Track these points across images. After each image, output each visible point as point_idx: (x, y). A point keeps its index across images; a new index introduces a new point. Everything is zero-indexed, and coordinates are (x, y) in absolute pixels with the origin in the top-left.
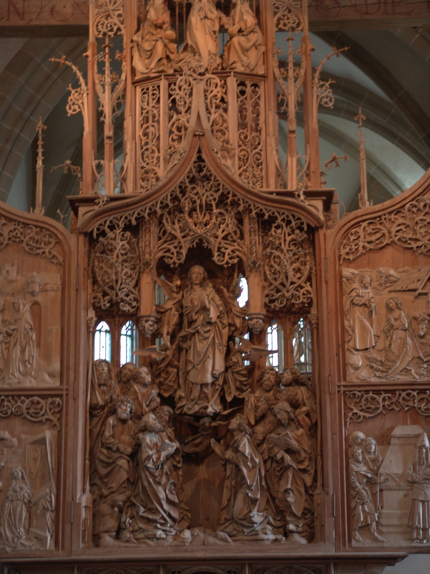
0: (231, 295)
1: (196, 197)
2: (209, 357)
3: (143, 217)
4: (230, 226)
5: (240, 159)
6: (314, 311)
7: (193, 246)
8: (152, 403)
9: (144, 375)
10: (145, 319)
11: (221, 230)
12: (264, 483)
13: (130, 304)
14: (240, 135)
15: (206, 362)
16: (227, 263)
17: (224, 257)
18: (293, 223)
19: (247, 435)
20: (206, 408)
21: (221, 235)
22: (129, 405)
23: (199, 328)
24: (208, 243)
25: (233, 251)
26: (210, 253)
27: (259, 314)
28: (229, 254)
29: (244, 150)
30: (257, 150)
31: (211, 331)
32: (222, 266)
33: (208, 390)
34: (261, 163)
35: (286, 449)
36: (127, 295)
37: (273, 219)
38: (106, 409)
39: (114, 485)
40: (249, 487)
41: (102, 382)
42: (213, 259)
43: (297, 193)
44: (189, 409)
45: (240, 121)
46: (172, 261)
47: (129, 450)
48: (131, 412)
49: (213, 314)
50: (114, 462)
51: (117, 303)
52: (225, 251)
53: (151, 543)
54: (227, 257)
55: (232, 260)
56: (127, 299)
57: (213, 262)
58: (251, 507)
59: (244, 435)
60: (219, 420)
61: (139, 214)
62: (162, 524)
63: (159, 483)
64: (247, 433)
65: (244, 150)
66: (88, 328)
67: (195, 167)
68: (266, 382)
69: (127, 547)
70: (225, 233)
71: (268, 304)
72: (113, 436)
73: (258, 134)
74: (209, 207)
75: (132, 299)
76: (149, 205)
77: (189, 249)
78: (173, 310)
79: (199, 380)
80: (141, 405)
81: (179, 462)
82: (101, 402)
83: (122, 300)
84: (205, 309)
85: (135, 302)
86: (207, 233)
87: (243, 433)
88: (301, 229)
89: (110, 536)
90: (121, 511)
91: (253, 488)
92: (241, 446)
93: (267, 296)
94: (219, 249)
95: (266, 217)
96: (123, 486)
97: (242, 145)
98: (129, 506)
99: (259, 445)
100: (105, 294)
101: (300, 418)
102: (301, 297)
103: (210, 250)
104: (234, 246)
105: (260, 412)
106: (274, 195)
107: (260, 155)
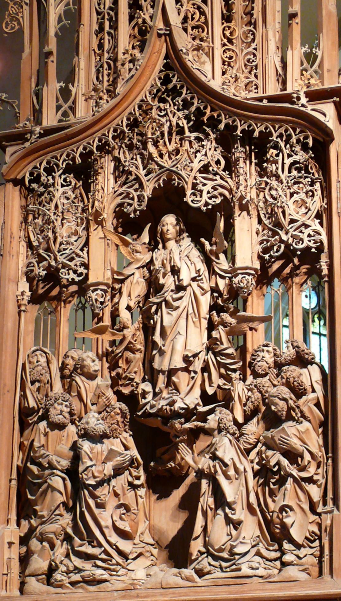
0: (214, 248)
1: (164, 120)
2: (179, 333)
3: (91, 152)
4: (209, 154)
5: (224, 62)
6: (324, 258)
7: (159, 185)
8: (100, 400)
9: (88, 362)
10: (92, 288)
11: (196, 161)
13: (75, 272)
14: (224, 29)
15: (175, 340)
16: (207, 204)
17: (201, 196)
18: (294, 140)
19: (228, 435)
21: (196, 165)
22: (67, 403)
23: (166, 294)
24: (179, 179)
25: (214, 188)
26: (182, 192)
27: (247, 268)
28: (208, 192)
29: (229, 50)
30: (250, 49)
31: (184, 298)
32: (199, 209)
33: (178, 378)
34: (256, 66)
36: (72, 259)
37: (265, 136)
39: (45, 513)
41: (36, 376)
42: (185, 199)
43: (295, 95)
44: (152, 407)
45: (225, 12)
46: (131, 209)
47: (65, 463)
48: (71, 414)
49: (186, 276)
50: (46, 482)
51: (57, 270)
52: (203, 188)
54: (205, 196)
55: (213, 199)
56: (72, 264)
57: (186, 203)
60: (195, 421)
61: (85, 148)
62: (103, 561)
63: (101, 506)
64: (228, 432)
65: (229, 50)
66: (19, 306)
67: (160, 78)
68: (259, 364)
70: (202, 163)
71: (261, 254)
73: (251, 28)
74: (181, 131)
75: (78, 264)
76: (99, 134)
77: (155, 188)
78: (137, 275)
79: (165, 368)
80: (85, 406)
81: (138, 478)
82: (32, 403)
83: (64, 266)
84: (175, 271)
85: (83, 268)
86: (178, 165)
87: (223, 433)
88: (305, 148)
89: (38, 580)
90: (52, 547)
93: (261, 243)
94: (194, 186)
95: (256, 134)
97: (227, 43)
99: (248, 452)
100: (41, 259)
101: (305, 409)
102: (306, 239)
103: (183, 187)
104: (216, 180)
106: (265, 101)
107: (255, 55)
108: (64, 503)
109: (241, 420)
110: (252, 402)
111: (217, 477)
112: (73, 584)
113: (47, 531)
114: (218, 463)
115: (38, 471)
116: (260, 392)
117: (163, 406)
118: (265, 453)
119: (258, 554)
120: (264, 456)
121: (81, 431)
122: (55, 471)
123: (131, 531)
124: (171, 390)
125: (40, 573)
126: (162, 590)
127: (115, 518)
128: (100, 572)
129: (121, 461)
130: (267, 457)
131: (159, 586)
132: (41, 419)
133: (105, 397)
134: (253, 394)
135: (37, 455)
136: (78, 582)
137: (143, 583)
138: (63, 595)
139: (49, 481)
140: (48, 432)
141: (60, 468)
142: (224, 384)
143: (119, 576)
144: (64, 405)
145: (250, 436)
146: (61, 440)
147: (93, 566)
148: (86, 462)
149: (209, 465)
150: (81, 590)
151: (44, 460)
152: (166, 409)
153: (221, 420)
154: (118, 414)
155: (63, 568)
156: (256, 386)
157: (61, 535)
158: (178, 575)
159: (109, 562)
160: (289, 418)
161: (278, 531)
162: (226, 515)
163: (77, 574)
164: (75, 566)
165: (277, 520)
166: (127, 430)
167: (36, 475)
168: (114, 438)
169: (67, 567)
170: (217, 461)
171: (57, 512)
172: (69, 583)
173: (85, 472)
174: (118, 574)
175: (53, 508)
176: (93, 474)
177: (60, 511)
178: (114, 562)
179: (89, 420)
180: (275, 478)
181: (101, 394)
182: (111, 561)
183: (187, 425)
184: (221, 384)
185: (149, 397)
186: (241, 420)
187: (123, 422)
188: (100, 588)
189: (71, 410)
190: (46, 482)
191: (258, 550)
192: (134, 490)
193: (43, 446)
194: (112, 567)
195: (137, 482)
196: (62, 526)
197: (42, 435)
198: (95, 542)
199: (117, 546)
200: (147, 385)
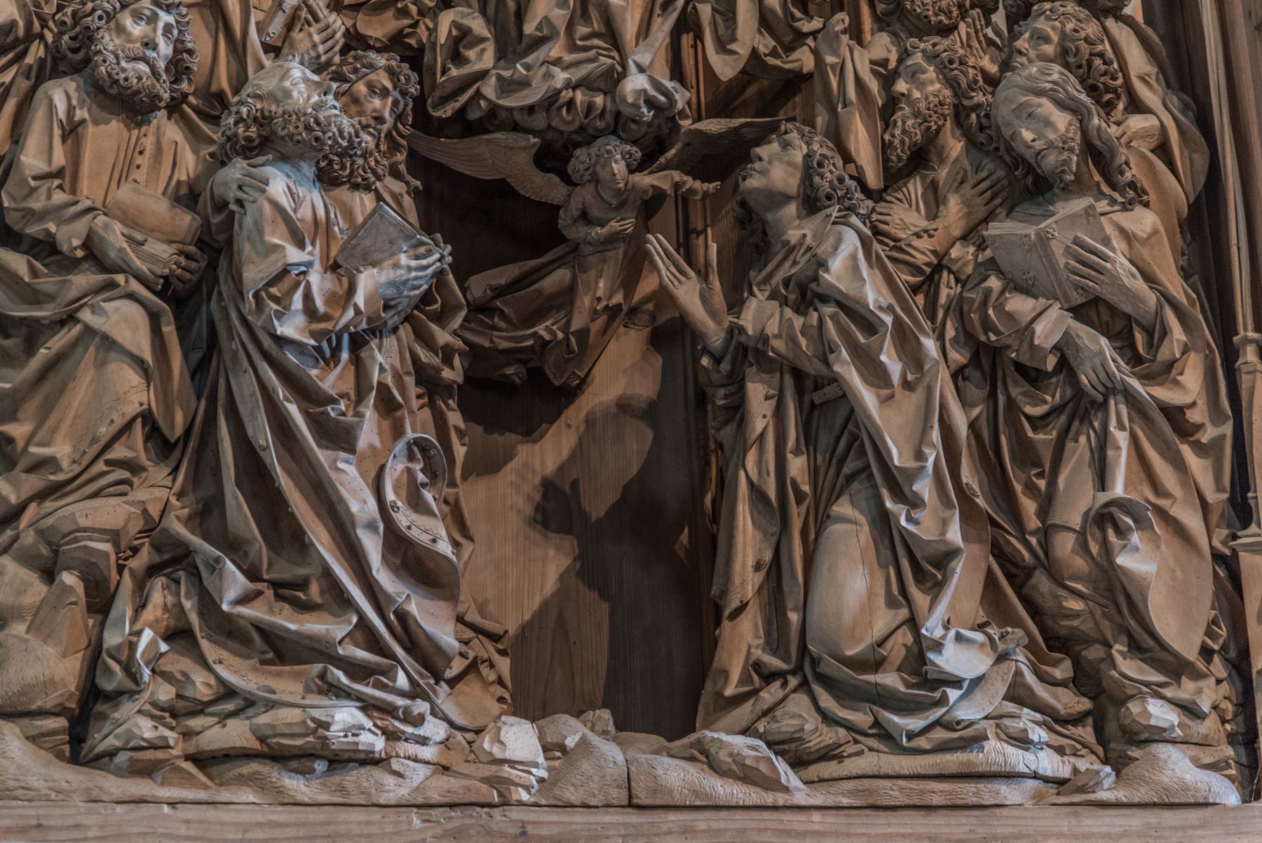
8: (297, 35)
12: (968, 475)
19: (854, 220)
20: (611, 80)
22: (170, 19)
35: (1078, 299)
38: (36, 52)
39: (62, 450)
40: (898, 484)
44: (508, 86)
48: (178, 68)
50: (70, 319)
53: (296, 785)
58: (920, 598)
59: (842, 221)
69: (141, 801)
72: (66, 176)
87: (834, 212)
91: (924, 487)
92: (837, 265)
96: (119, 452)
98: (153, 571)
105: (907, 125)
108: (146, 416)
109: (873, 179)
110: (917, 114)
111: (837, 368)
112: (204, 761)
113: (83, 522)
114: (832, 317)
115: (34, 273)
116: (952, 83)
117: (569, 85)
118: (999, 308)
119: (1018, 695)
120: (991, 312)
121: (247, 129)
122: (120, 278)
123: (454, 558)
124: (582, 39)
125: (50, 702)
126: (634, 818)
127: (390, 496)
128: (345, 716)
129: (409, 269)
130: (1010, 316)
131: (619, 795)
132: (54, 67)
133: (322, 24)
134: (921, 86)
135: (37, 204)
136: (246, 755)
137: (541, 781)
138: (166, 809)
139: (86, 316)
140: (83, 122)
141: (138, 264)
142: (774, 53)
143: (423, 741)
144: (161, 25)
145: (916, 242)
146: (130, 165)
147: (308, 690)
148: (276, 248)
149: (786, 325)
150: (247, 795)
151: (65, 229)
152: (570, 103)
153: (820, 165)
154: (384, 93)
155: (165, 693)
156: (932, 57)
157: (135, 550)
158: (696, 753)
159: (382, 679)
160: (1078, 186)
161: (1075, 605)
162: (883, 522)
163: (231, 723)
164: (221, 681)
165: (1080, 564)
166: (402, 167)
167: (27, 284)
168: (355, 187)
169: (180, 681)
170: (828, 310)
171: (119, 452)
172: (188, 758)
173: (274, 290)
174: (421, 731)
175: (105, 431)
176: (308, 297)
177: (131, 449)
178: (402, 681)
179: (287, 84)
180: (1046, 402)
181: (304, 14)
182: (388, 672)
183: (645, 180)
184: (762, 49)
185: (483, 58)
186: (873, 179)
187: (389, 134)
188: (342, 789)
189: (176, 51)
190: (70, 319)
191: (1018, 673)
192: (432, 404)
193: (59, 174)
194: (400, 702)
195: (447, 374)
196: (145, 511)
197: (57, 132)
198: (315, 590)
199: (403, 616)
200: (464, 15)
